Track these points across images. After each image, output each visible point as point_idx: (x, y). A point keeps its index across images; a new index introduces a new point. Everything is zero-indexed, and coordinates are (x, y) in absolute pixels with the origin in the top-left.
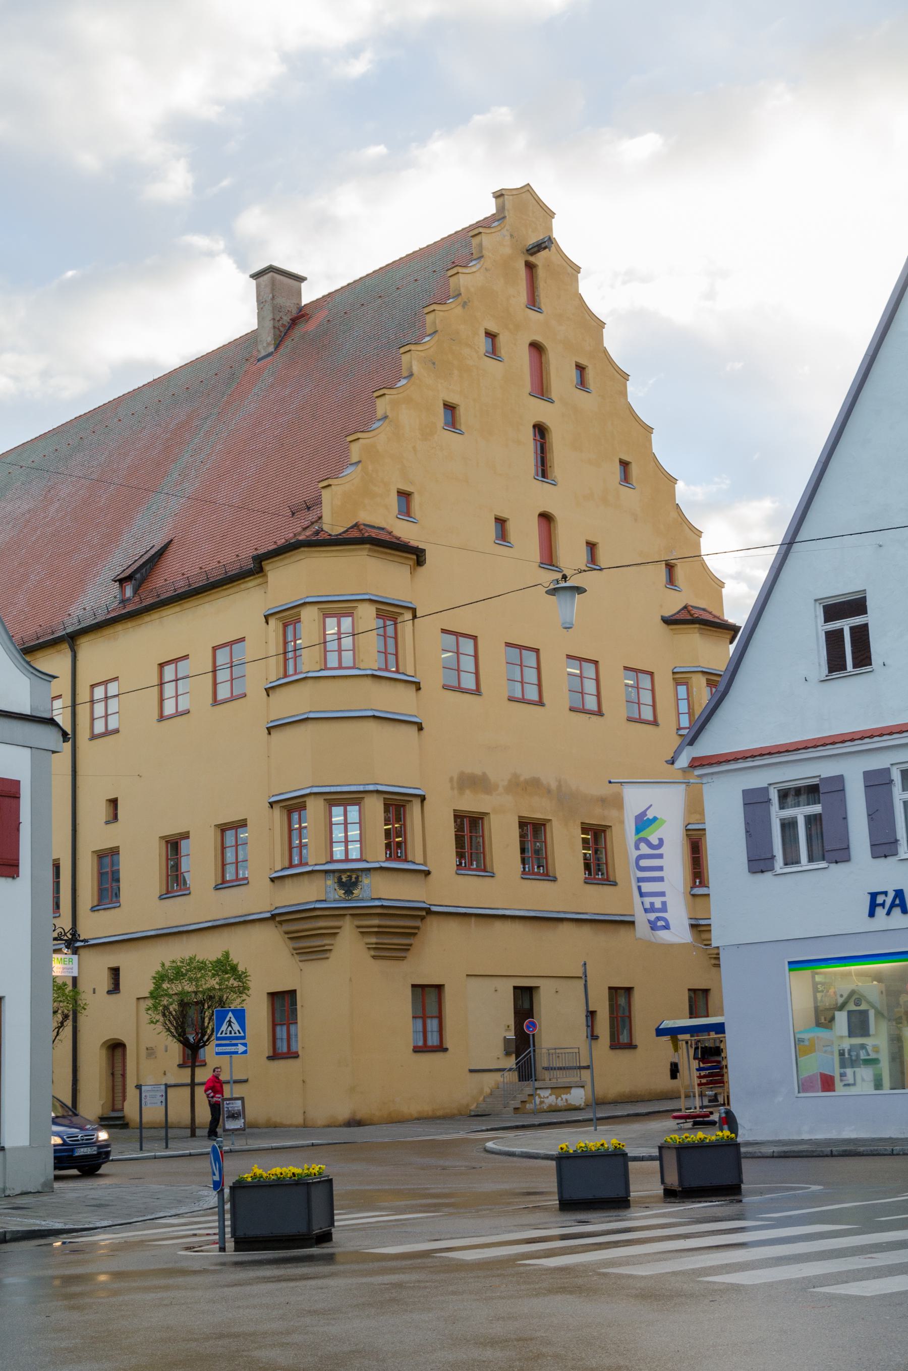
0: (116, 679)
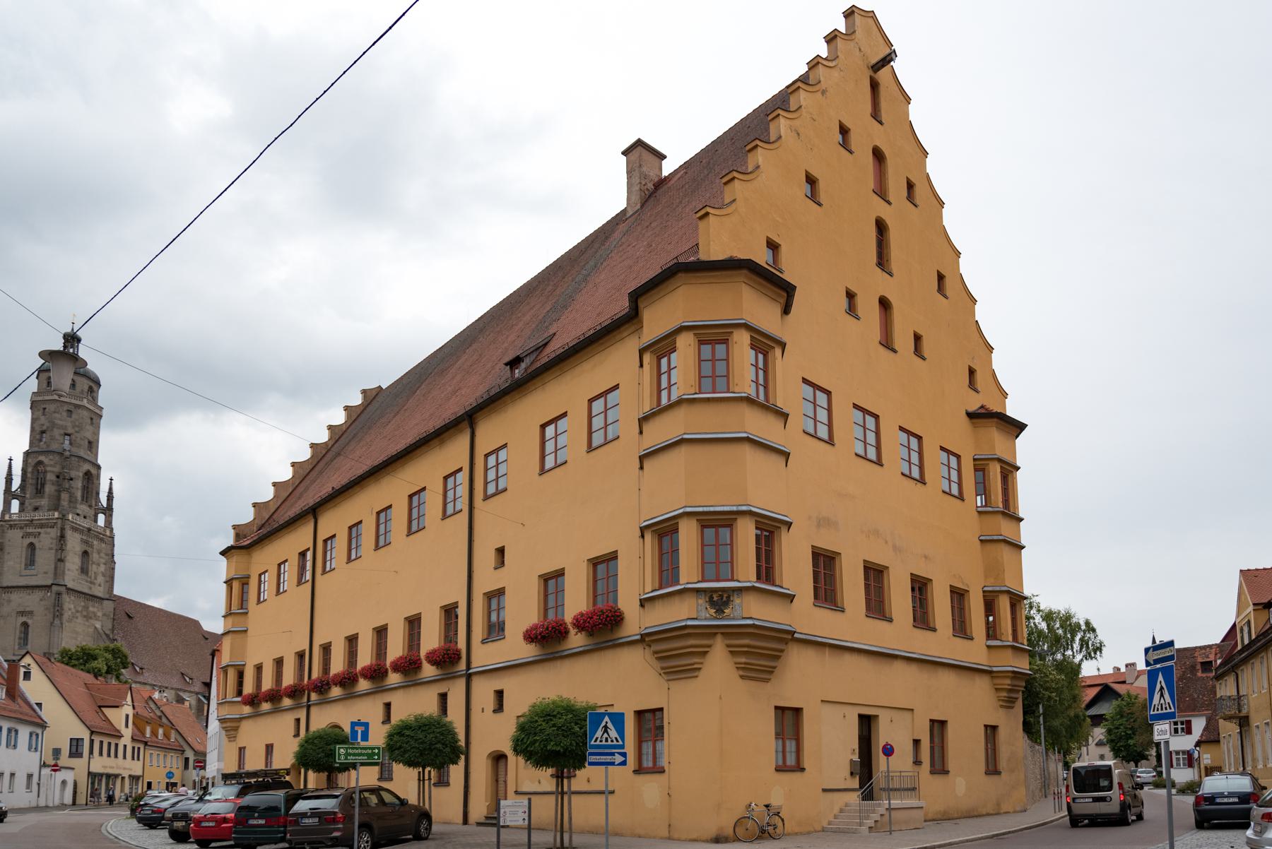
0: (505, 446)
